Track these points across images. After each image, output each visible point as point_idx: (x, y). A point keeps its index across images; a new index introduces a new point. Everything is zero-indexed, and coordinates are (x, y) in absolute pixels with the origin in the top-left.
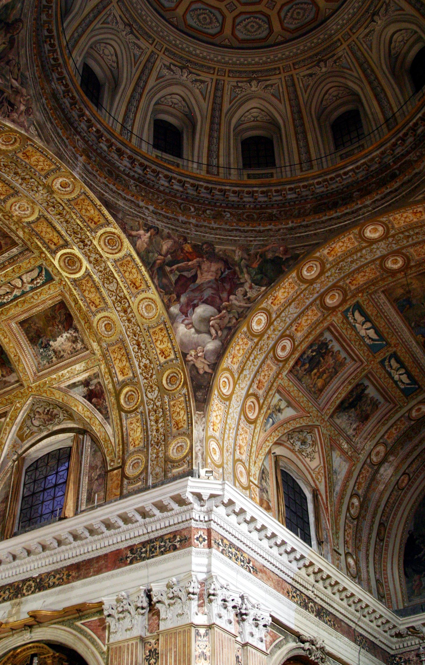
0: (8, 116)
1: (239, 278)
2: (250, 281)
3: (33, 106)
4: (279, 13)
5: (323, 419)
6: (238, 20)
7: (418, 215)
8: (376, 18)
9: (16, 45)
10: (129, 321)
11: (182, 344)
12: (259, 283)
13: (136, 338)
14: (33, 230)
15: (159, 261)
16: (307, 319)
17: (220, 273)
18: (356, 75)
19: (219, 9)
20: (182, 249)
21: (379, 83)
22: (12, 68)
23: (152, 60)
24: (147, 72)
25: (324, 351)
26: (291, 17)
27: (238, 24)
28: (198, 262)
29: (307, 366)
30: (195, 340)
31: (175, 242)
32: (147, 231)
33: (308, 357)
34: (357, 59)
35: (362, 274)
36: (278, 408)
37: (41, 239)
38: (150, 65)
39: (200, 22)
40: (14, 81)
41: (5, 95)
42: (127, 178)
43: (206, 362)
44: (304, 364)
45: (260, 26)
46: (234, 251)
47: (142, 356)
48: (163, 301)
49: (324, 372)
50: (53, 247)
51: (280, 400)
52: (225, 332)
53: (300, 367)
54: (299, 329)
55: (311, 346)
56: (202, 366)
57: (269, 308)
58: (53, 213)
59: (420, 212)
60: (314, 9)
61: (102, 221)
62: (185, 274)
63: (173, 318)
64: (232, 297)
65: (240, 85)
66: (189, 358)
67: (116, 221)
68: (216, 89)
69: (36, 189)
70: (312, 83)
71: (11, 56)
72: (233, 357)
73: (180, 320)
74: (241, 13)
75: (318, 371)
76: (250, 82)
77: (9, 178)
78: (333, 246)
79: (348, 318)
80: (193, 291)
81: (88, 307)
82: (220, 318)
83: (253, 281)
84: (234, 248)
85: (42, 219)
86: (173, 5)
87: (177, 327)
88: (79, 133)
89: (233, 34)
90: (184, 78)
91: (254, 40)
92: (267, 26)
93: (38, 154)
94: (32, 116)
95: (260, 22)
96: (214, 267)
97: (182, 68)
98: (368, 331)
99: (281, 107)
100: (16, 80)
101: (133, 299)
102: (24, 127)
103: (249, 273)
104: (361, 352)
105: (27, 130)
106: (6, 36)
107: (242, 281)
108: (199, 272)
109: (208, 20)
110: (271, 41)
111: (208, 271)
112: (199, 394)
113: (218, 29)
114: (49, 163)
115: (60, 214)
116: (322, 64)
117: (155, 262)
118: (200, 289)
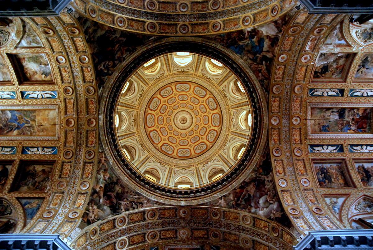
1: (262, 180)
2: (265, 177)
4: (213, 126)
6: (207, 139)
7: (276, 100)
8: (226, 96)
9: (125, 187)
10: (248, 231)
11: (266, 217)
12: (268, 174)
13: (255, 234)
14: (195, 237)
15: (234, 203)
16: (300, 167)
17: (255, 186)
18: (239, 110)
19: (201, 142)
20: (237, 193)
21: (243, 102)
23: (198, 169)
24: (199, 173)
25: (325, 171)
26: (216, 122)
28: (246, 190)
29: (327, 181)
30: (269, 211)
31: (233, 193)
32: (221, 199)
33: (322, 178)
34: (236, 107)
35: (295, 135)
37: (200, 237)
38: (198, 171)
41: (135, 202)
43: (279, 212)
44: (325, 182)
45: (213, 134)
46: (252, 175)
47: (263, 237)
49: (337, 177)
50: (206, 236)
52: (275, 198)
54: (302, 172)
55: (317, 174)
56: (279, 215)
58: (193, 225)
59: (275, 99)
60: (217, 114)
61: (206, 211)
62: (245, 198)
63: (255, 213)
64: (266, 187)
66: (272, 218)
68: (220, 157)
69: (179, 223)
70: (236, 126)
71: (126, 190)
72: (287, 201)
74: (206, 137)
75: (334, 178)
77: (169, 228)
78: (273, 139)
79: (314, 152)
80: (253, 199)
81: (235, 243)
82: (269, 196)
83: (266, 175)
84: (251, 175)
85: (193, 230)
86: (190, 154)
87: (259, 214)
90: (210, 164)
91: (216, 138)
93: (166, 211)
96: (251, 186)
97: (207, 163)
98: (329, 149)
99: (237, 140)
100: (135, 195)
101: (240, 223)
102: (152, 206)
103: (262, 175)
104: (337, 156)
105: (154, 206)
106: (118, 186)
107: (263, 179)
108: (249, 193)
109: (202, 147)
110: (219, 132)
112: (286, 223)
113: (206, 146)
114: (172, 210)
116: (233, 120)
117: (233, 204)
118: (254, 196)
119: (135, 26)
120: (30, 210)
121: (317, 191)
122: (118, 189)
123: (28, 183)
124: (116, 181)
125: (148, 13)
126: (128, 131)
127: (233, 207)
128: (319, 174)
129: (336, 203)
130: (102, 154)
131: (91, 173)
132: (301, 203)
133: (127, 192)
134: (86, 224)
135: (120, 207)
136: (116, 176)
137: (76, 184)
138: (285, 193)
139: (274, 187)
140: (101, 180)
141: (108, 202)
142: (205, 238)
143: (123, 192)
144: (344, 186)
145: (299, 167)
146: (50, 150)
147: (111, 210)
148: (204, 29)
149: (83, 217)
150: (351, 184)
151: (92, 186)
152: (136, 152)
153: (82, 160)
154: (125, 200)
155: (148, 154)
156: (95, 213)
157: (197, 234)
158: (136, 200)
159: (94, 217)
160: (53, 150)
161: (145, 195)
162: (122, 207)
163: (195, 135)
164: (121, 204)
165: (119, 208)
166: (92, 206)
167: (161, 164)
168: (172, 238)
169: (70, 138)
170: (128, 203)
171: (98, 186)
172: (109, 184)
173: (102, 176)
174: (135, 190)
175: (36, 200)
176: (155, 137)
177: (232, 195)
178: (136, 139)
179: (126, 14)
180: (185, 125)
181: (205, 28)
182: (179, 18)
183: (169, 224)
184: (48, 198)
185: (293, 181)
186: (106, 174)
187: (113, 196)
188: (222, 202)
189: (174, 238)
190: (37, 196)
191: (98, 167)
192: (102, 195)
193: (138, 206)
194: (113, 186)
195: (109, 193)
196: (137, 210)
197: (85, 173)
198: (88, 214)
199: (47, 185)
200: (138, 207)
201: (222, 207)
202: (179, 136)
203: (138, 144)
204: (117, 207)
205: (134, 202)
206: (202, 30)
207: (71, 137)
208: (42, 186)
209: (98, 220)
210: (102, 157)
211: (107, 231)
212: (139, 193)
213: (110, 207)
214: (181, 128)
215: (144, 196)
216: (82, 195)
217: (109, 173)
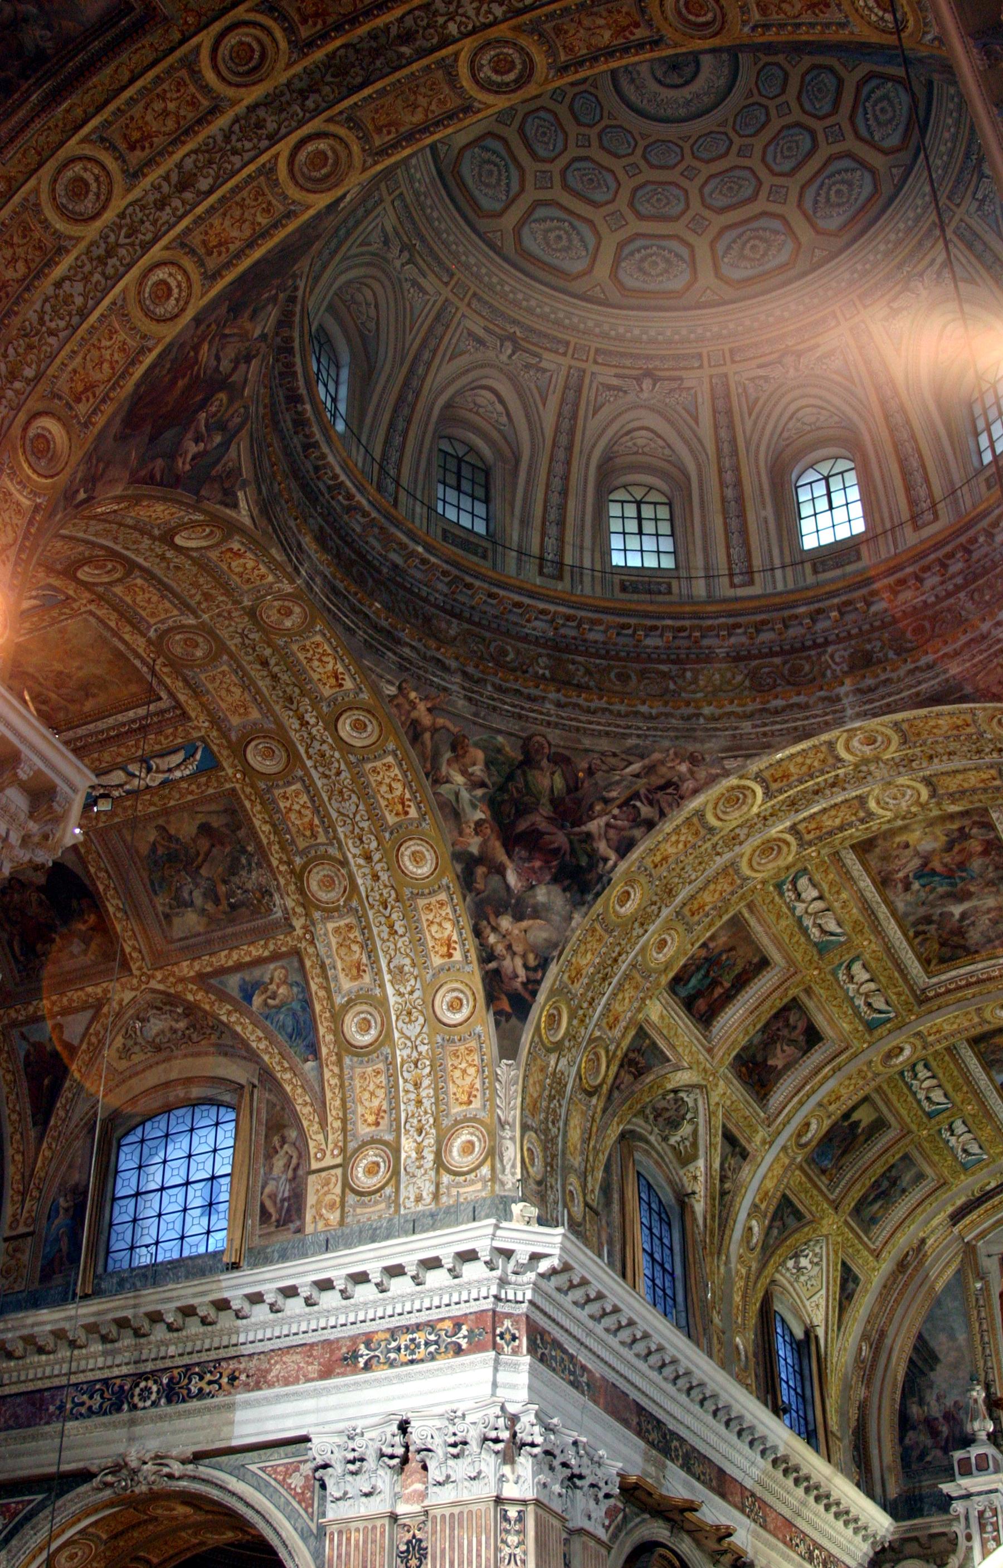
0: (682, 798)
3: (691, 748)
6: (863, 131)
9: (567, 753)
22: (604, 767)
27: (871, 134)
37: (974, 791)
39: (839, 205)
40: (628, 770)
41: (643, 791)
42: (952, 601)
45: (885, 97)
65: (979, 196)
67: (974, 701)
71: (585, 765)
74: (852, 119)
76: (982, 176)
88: (827, 643)
89: (886, 152)
92: (890, 84)
94: (708, 758)
95: (879, 93)
100: (630, 763)
102: (717, 776)
105: (727, 774)
109: (844, 188)
115: (931, 757)
119: (235, 233)
123: (186, 895)
124: (521, 758)
125: (252, 109)
126: (409, 338)
130: (406, 696)
131: (408, 796)
133: (590, 772)
134: (514, 1020)
135: (595, 851)
136: (511, 734)
137: (376, 857)
140: (465, 795)
141: (537, 864)
143: (572, 784)
146: (178, 758)
147: (564, 890)
148: (624, 29)
149: (491, 998)
151: (446, 852)
152: (501, 400)
153: (337, 755)
154: (598, 808)
155: (565, 361)
156: (518, 948)
157: (953, 784)
158: (641, 785)
159: (525, 966)
160: (193, 755)
162: (602, 847)
163: (776, 124)
164: (589, 835)
165: (595, 859)
166: (495, 929)
167: (656, 380)
169: (228, 691)
170: (615, 817)
171: (469, 830)
172: (502, 788)
173: (459, 779)
175: (272, 966)
176: (559, 238)
178: (471, 334)
179: (154, 223)
180: (696, 87)
181: (624, 22)
182: (441, 20)
183: (816, 793)
184: (311, 950)
186: (467, 760)
187: (543, 826)
190: (266, 953)
191: (422, 756)
192: (502, 856)
193: (664, 805)
194: (521, 785)
195: (522, 826)
196: (668, 827)
197: (383, 803)
198: (497, 972)
200: (666, 810)
202: (688, 159)
203: (491, 354)
204: (584, 862)
205: (636, 796)
206: (616, 35)
207: (233, 689)
208: (246, 891)
209: (544, 964)
210: (413, 706)
212: (637, 746)
213: (555, 880)
214: (682, 112)
216: (433, 900)
217: (476, 745)
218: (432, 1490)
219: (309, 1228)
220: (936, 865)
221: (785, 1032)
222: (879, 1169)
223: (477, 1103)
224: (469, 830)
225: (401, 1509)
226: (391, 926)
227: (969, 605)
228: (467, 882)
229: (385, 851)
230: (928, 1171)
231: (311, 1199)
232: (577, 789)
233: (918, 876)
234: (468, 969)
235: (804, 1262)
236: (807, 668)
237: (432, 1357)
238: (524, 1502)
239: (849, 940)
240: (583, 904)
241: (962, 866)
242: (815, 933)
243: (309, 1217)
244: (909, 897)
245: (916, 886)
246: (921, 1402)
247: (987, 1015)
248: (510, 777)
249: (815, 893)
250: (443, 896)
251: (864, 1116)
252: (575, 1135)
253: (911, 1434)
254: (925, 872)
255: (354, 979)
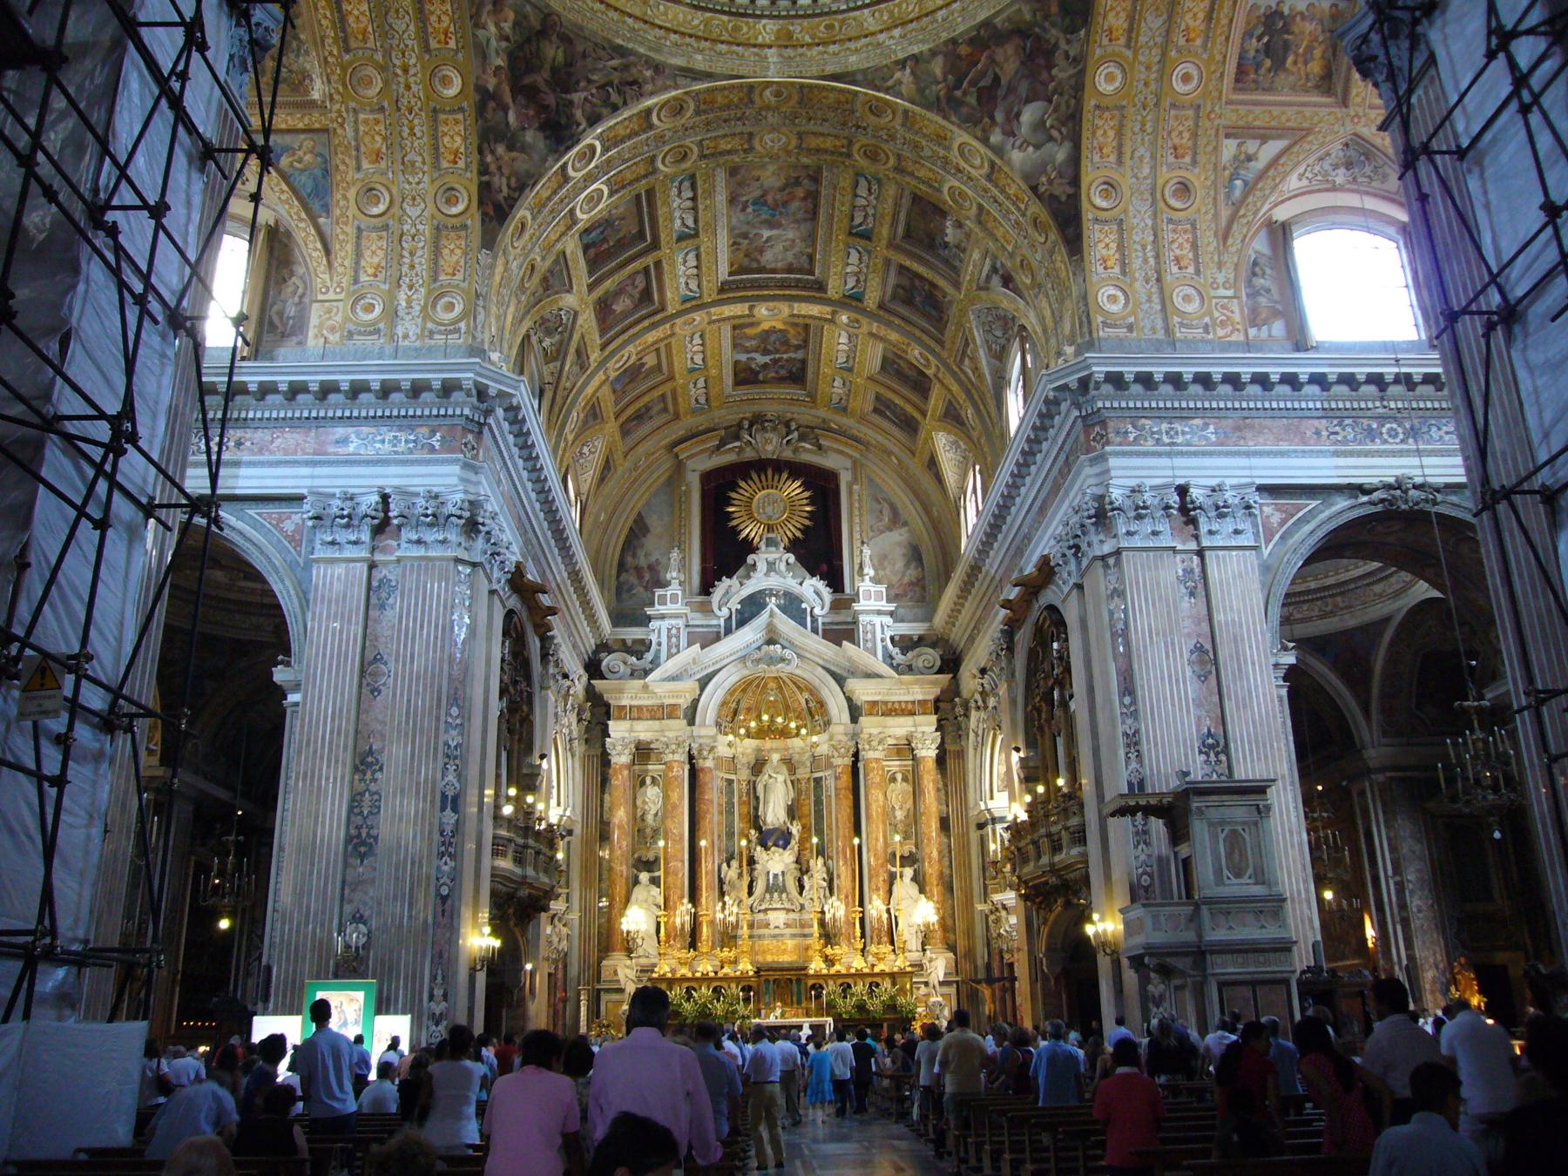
1: (1047, 41)
2: (1061, 36)
5: (1357, 115)
11: (1026, 177)
12: (1073, 30)
14: (809, 150)
20: (959, 56)
28: (989, 57)
29: (1268, 63)
32: (904, 67)
36: (1242, 157)
37: (826, 151)
41: (616, 82)
44: (1258, 66)
48: (976, 137)
49: (1310, 49)
51: (1239, 145)
52: (1070, 125)
53: (1256, 72)
54: (1192, 35)
55: (1248, 34)
57: (1109, 49)
62: (982, 84)
63: (999, 151)
64: (1054, 71)
66: (1042, 189)
71: (580, 48)
73: (1009, 147)
75: (1297, 55)
80: (1005, 97)
82: (1055, 110)
88: (762, 17)
96: (1010, 49)
103: (1053, 25)
105: (676, 88)
107: (1053, 41)
111: (1007, 60)
117: (938, 99)
120: (303, 178)
121: (1212, 111)
122: (553, 52)
127: (935, 105)
128: (1251, 36)
129: (1249, 159)
132: (1141, 158)
134: (495, 223)
135: (573, 115)
137: (412, 71)
138: (1107, 114)
139: (1078, 87)
140: (494, 43)
142: (841, 154)
144: (1317, 87)
145: (1188, 16)
149: (481, 203)
150: (1339, 90)
151: (472, 81)
154: (583, 84)
156: (506, 171)
157: (814, 142)
158: (616, 77)
161: (642, 50)
162: (578, 114)
164: (571, 103)
166: (493, 152)
168: (736, 151)
172: (520, 47)
173: (493, 29)
174: (609, 41)
177: (939, 60)
184: (339, 131)
185: (1148, 68)
188: (905, 77)
189: (745, 151)
190: (301, 126)
192: (508, 98)
195: (527, 80)
197: (430, 30)
199: (308, 67)
201: (899, 95)
205: (610, 84)
211: (549, 199)
213: (542, 128)
215: (642, 56)
218: (404, 545)
219: (311, 342)
220: (770, 199)
221: (629, 289)
222: (646, 399)
223: (459, 276)
224: (490, 71)
225: (378, 557)
226: (412, 129)
227: (870, 19)
228: (481, 109)
229: (423, 67)
230: (671, 407)
231: (314, 320)
232: (571, 65)
233: (754, 203)
234: (468, 175)
235: (586, 450)
236: (745, 29)
237: (411, 452)
238: (474, 565)
239: (696, 235)
240: (556, 151)
241: (785, 204)
242: (678, 222)
243: (311, 334)
244: (742, 217)
245: (750, 210)
246: (634, 556)
247: (756, 311)
248: (528, 40)
249: (690, 195)
250: (460, 117)
251: (650, 360)
252: (510, 318)
253: (624, 576)
254: (760, 201)
255: (372, 162)
